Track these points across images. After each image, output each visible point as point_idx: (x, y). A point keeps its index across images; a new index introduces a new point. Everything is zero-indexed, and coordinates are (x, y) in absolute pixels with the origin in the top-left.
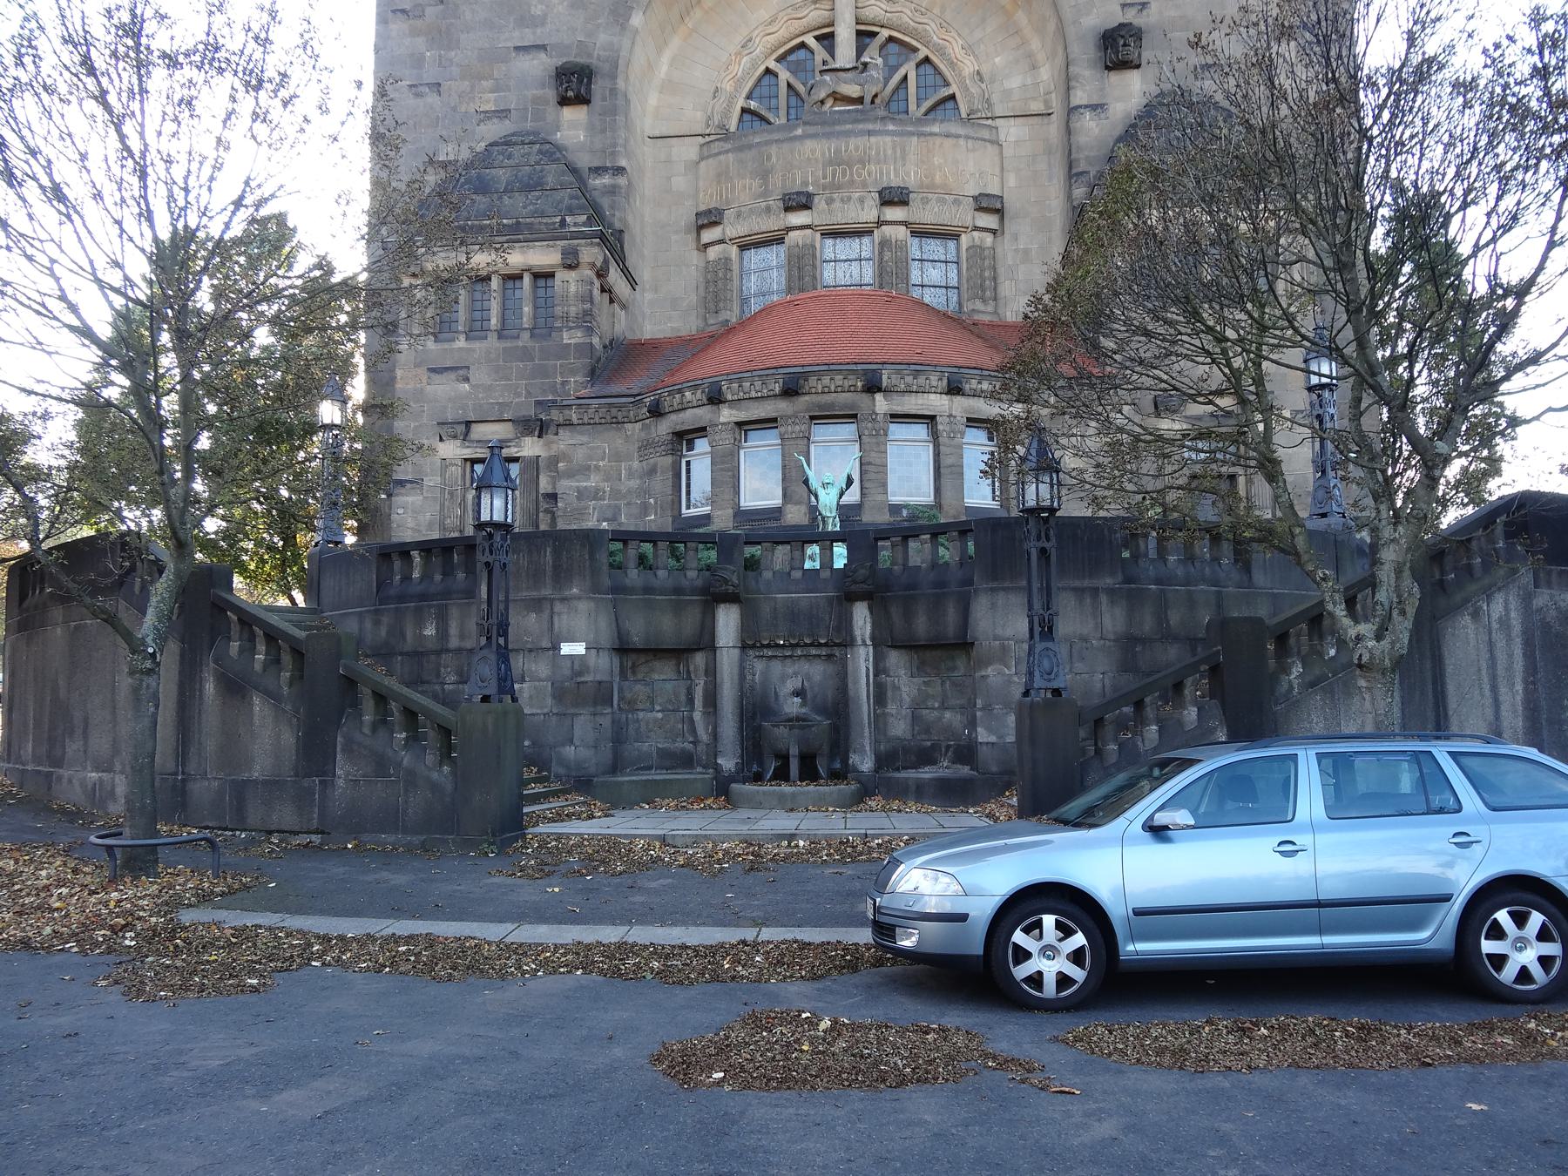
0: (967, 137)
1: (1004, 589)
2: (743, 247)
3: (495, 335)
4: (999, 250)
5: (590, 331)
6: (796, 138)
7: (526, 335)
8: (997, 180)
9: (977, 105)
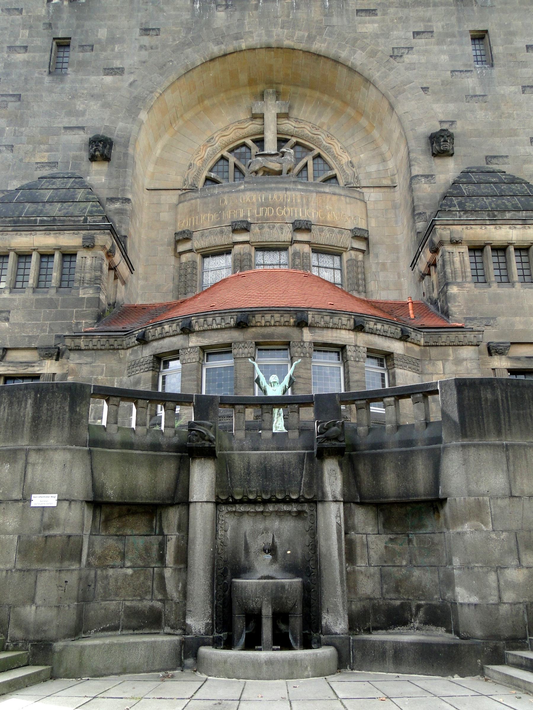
0: (346, 196)
1: (474, 446)
2: (205, 256)
3: (31, 290)
4: (367, 265)
5: (99, 290)
7: (53, 291)
8: (364, 222)
9: (350, 180)
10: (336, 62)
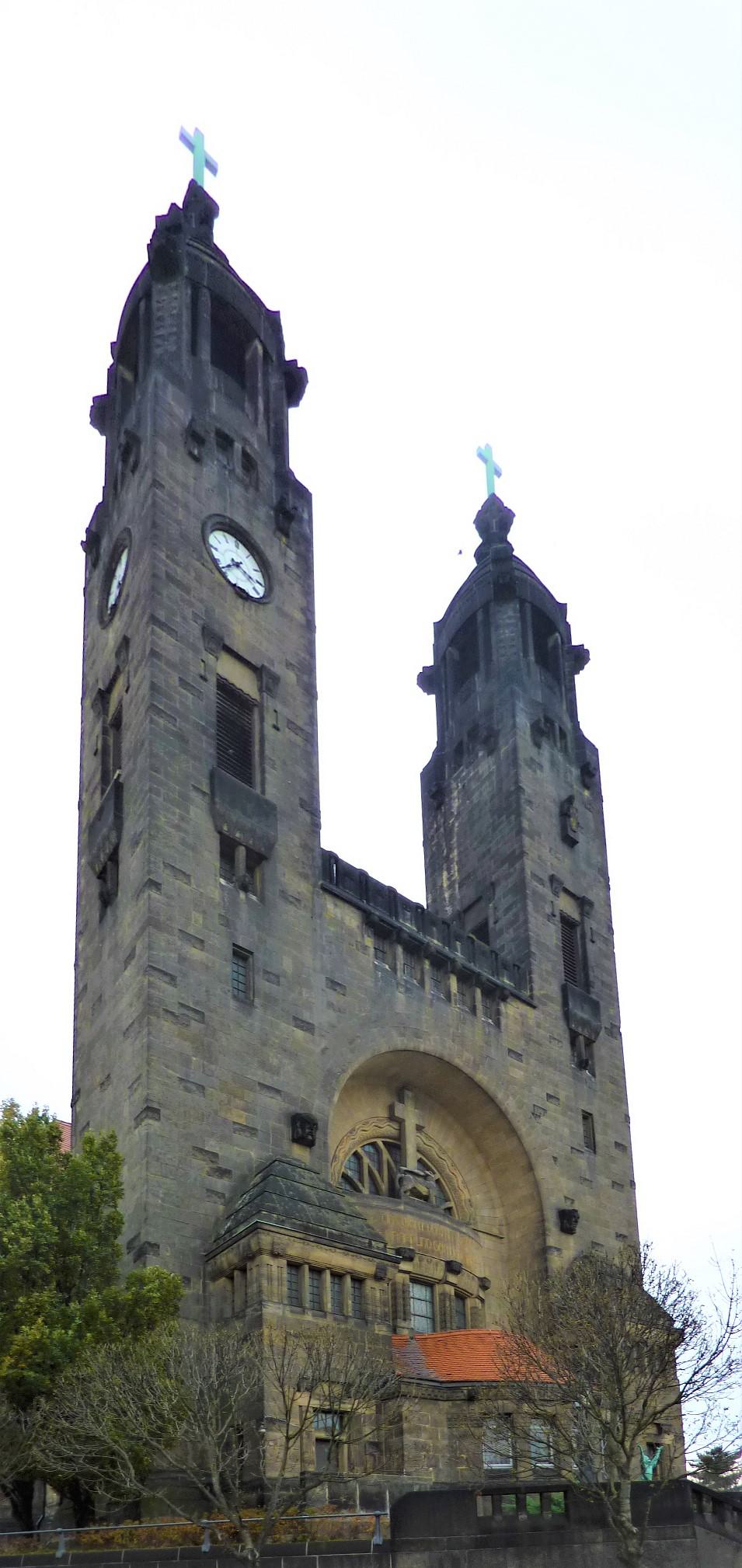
6: (399, 1211)
10: (491, 1100)
